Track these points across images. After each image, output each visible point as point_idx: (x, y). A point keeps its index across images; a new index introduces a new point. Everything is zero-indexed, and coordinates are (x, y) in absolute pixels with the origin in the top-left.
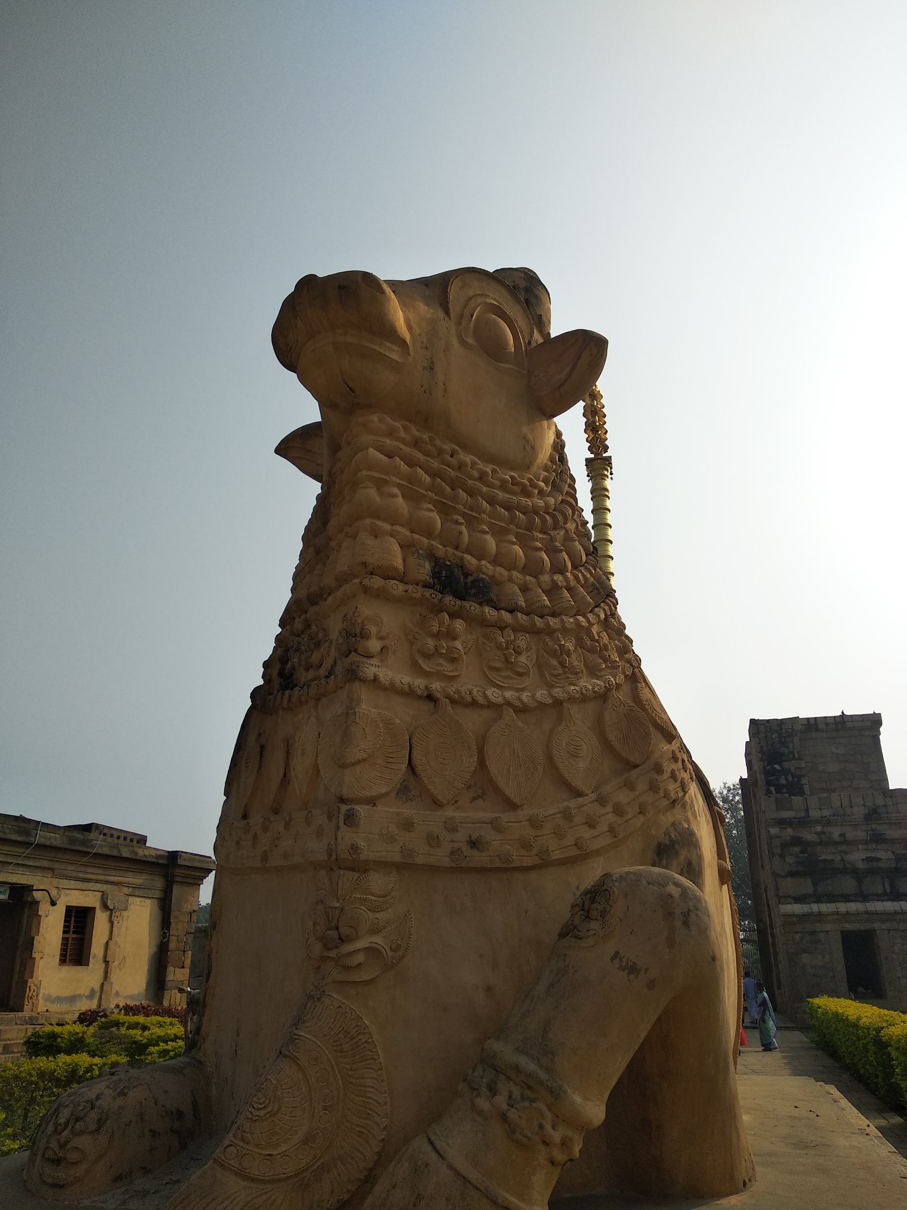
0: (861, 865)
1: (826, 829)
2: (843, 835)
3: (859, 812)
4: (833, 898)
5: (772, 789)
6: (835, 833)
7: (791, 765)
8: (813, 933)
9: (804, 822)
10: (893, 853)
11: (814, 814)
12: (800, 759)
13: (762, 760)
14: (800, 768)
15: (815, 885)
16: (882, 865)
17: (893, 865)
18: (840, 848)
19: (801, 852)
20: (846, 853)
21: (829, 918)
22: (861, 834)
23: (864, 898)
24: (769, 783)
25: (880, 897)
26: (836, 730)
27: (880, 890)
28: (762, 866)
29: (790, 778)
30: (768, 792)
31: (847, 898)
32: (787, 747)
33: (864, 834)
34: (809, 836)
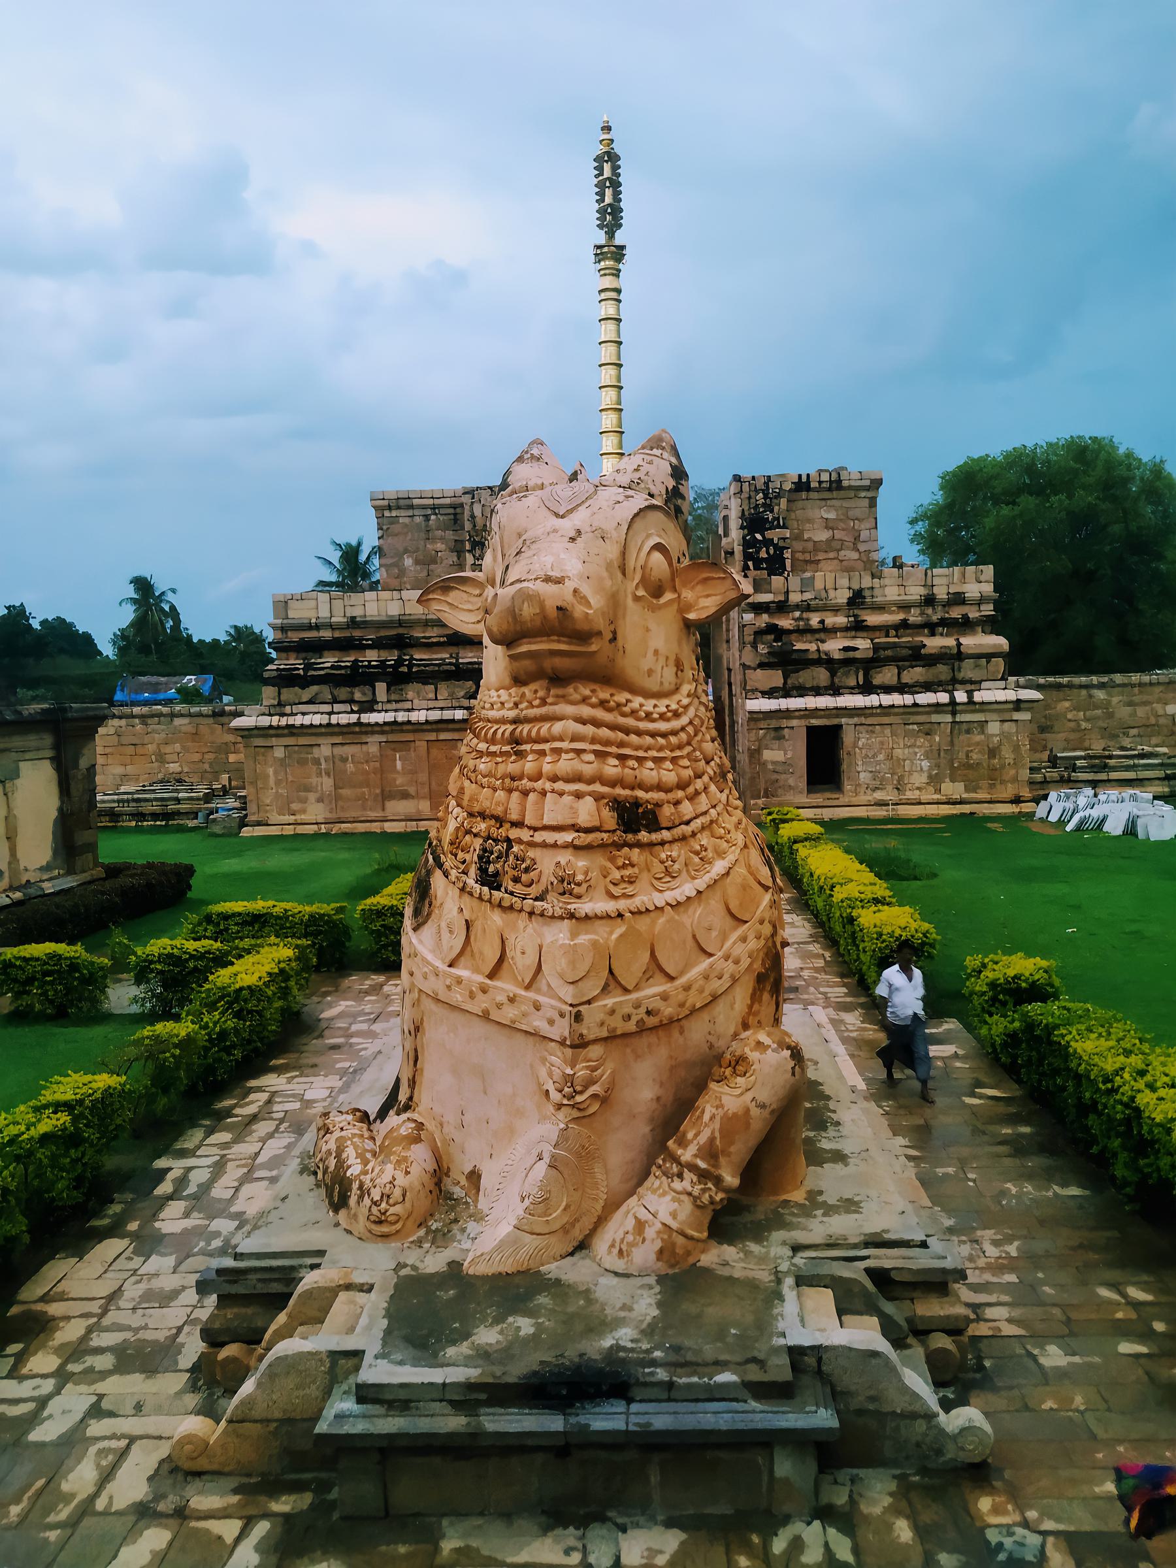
0: (837, 656)
1: (805, 615)
2: (822, 622)
3: (842, 596)
4: (802, 691)
5: (750, 563)
6: (814, 620)
7: (774, 535)
8: (778, 729)
9: (782, 607)
10: (872, 640)
11: (795, 598)
12: (784, 527)
13: (742, 528)
14: (784, 539)
15: (786, 678)
16: (858, 655)
17: (870, 654)
18: (817, 636)
19: (775, 641)
20: (823, 641)
21: (797, 714)
22: (841, 620)
23: (836, 691)
24: (747, 556)
25: (852, 690)
26: (830, 489)
27: (853, 683)
28: (728, 641)
29: (772, 552)
30: (745, 568)
31: (817, 691)
32: (772, 511)
33: (845, 620)
34: (785, 623)
